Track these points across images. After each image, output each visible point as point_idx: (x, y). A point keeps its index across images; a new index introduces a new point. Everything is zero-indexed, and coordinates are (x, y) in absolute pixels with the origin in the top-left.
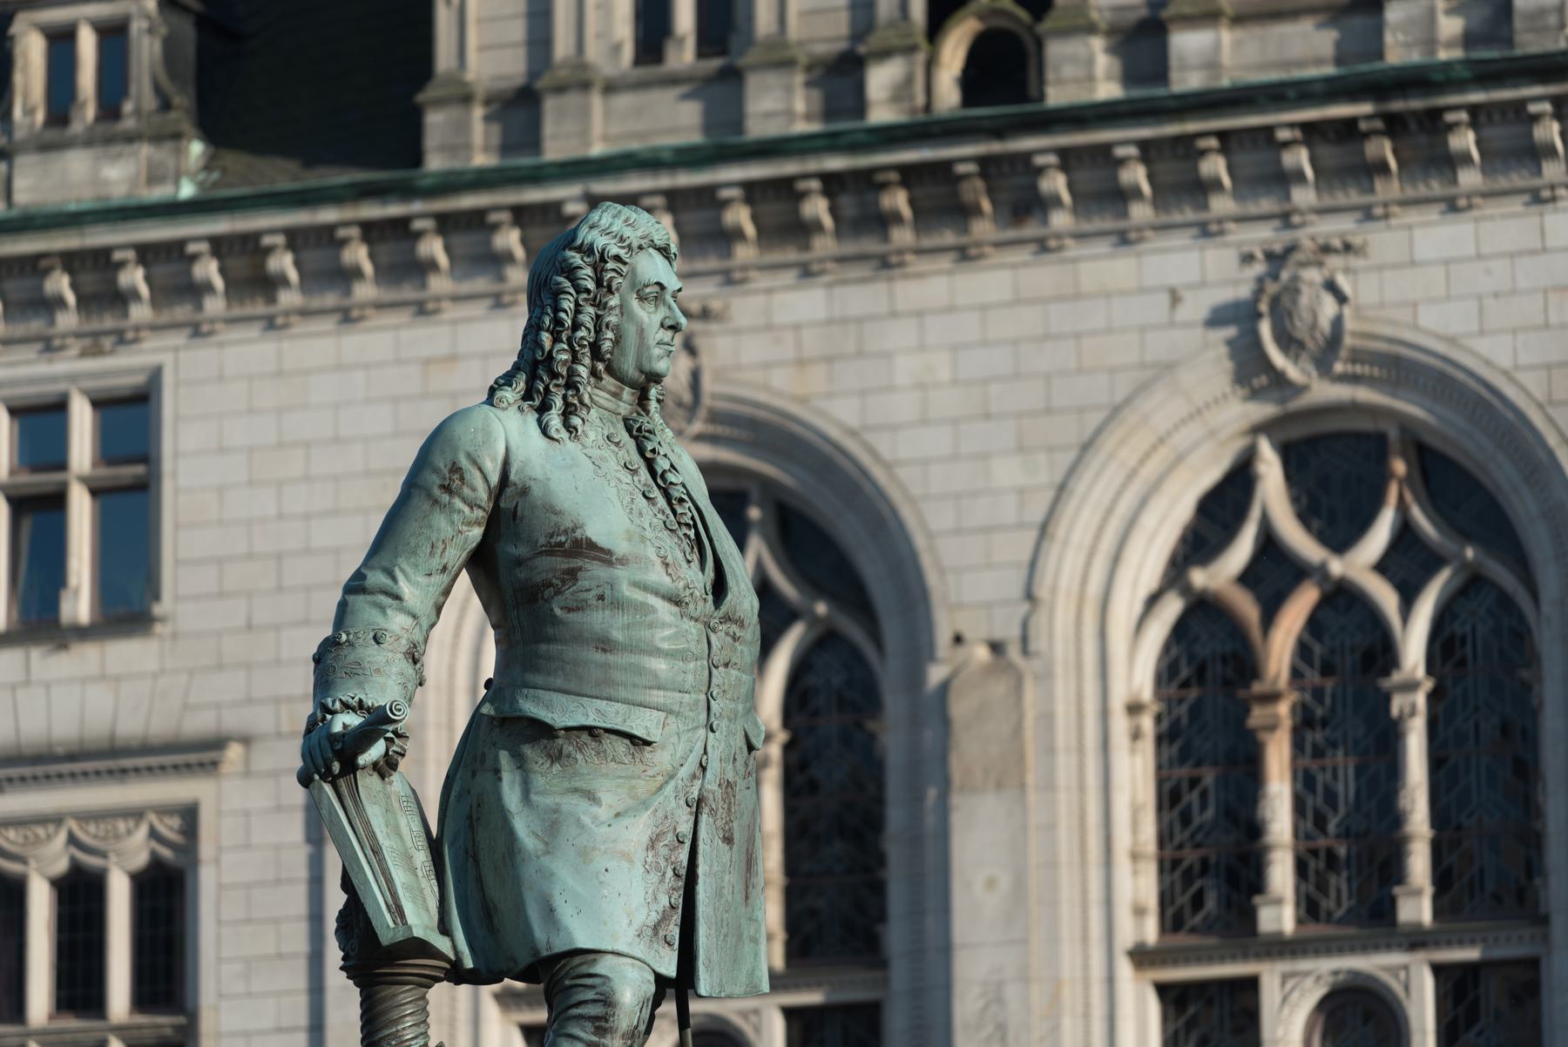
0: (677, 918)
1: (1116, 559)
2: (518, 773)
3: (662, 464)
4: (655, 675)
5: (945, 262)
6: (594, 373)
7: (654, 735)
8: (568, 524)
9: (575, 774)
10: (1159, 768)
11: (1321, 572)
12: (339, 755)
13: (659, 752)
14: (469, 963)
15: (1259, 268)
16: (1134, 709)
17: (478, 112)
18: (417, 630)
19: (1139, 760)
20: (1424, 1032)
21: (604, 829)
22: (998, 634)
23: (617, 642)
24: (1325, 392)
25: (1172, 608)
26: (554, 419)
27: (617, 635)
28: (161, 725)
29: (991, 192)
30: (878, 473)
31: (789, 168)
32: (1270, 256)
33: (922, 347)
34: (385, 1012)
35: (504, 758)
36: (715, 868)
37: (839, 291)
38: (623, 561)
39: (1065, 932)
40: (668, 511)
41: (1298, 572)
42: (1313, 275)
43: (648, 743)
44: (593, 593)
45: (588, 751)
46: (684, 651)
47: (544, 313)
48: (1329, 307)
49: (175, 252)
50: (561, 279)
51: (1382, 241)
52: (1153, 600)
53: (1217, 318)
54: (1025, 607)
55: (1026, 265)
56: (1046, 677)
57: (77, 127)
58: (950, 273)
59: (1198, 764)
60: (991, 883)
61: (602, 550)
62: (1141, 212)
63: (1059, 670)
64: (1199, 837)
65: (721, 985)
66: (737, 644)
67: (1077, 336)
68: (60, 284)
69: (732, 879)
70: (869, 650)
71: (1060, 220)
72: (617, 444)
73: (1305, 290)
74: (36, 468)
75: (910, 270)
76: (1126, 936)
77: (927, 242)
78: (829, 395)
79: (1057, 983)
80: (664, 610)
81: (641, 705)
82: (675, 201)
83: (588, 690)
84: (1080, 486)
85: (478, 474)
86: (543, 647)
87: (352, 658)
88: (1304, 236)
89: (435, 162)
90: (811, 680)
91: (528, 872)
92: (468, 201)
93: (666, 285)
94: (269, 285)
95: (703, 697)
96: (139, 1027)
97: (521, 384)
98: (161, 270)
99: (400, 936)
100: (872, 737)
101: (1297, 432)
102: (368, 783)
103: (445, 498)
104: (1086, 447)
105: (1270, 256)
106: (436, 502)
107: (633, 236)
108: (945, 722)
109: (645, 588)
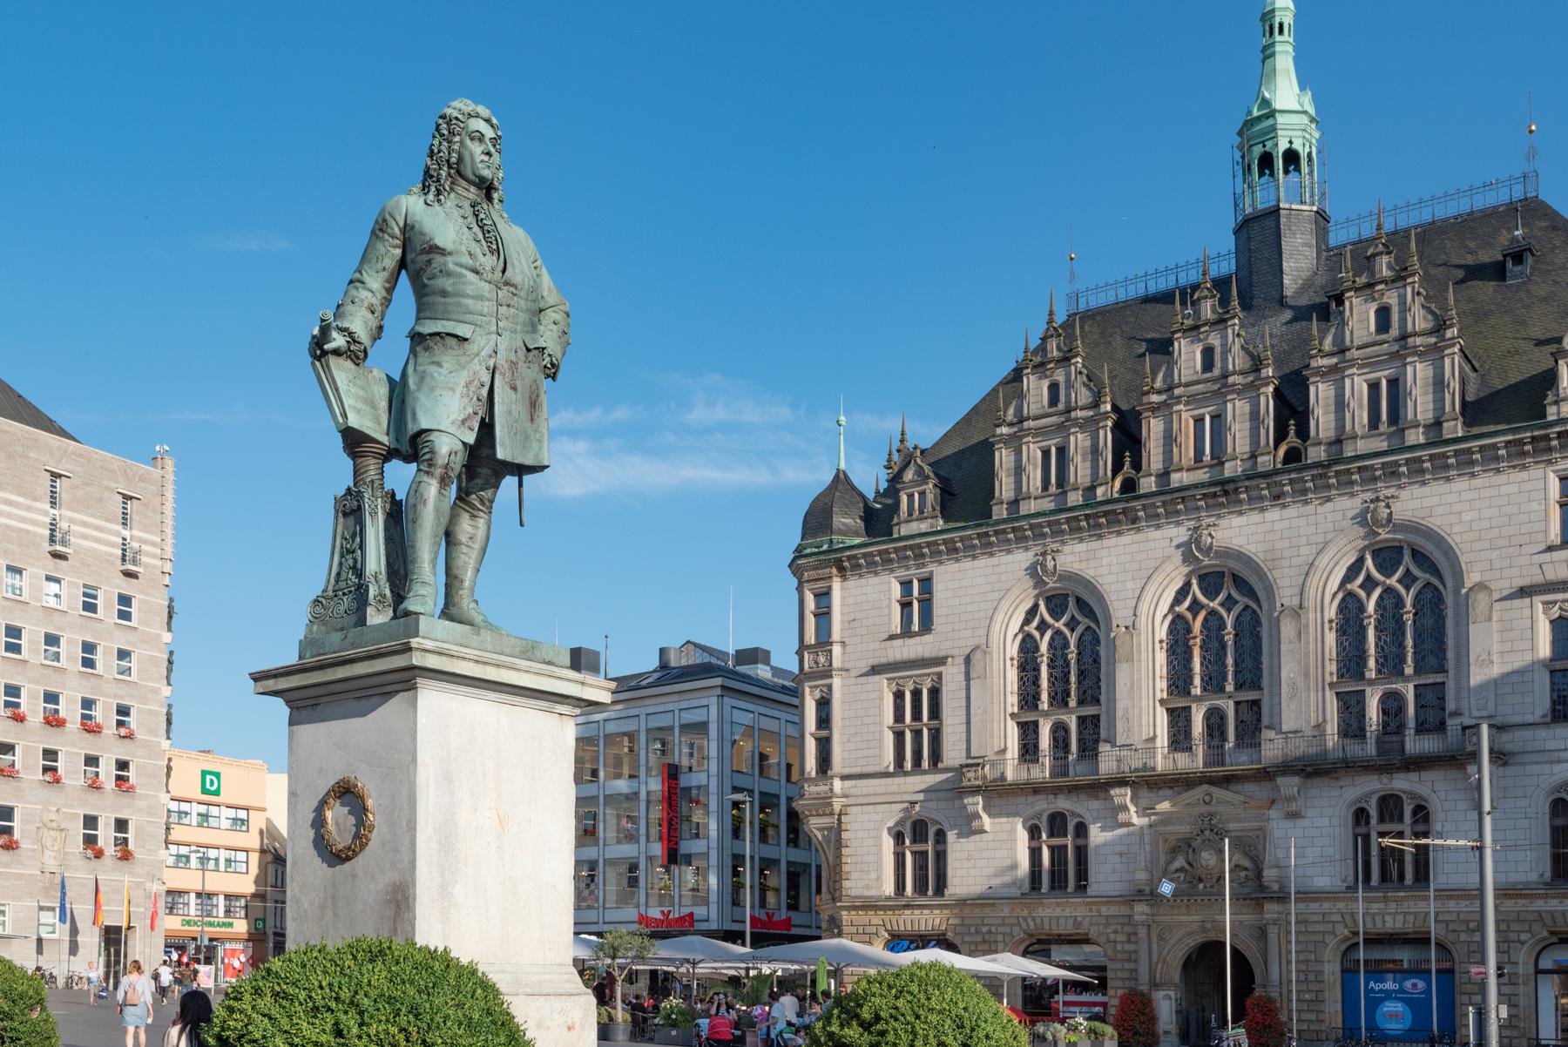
11: (1208, 605)
15: (1190, 533)
17: (1005, 506)
24: (1207, 562)
28: (934, 654)
30: (1099, 587)
41: (1202, 607)
42: (1205, 532)
43: (466, 340)
48: (1209, 540)
51: (1223, 523)
53: (1178, 547)
56: (1139, 635)
57: (914, 516)
60: (1125, 684)
76: (1159, 696)
83: (439, 316)
84: (1147, 588)
86: (425, 299)
88: (1203, 523)
89: (994, 518)
90: (1083, 638)
95: (494, 320)
108: (1115, 646)
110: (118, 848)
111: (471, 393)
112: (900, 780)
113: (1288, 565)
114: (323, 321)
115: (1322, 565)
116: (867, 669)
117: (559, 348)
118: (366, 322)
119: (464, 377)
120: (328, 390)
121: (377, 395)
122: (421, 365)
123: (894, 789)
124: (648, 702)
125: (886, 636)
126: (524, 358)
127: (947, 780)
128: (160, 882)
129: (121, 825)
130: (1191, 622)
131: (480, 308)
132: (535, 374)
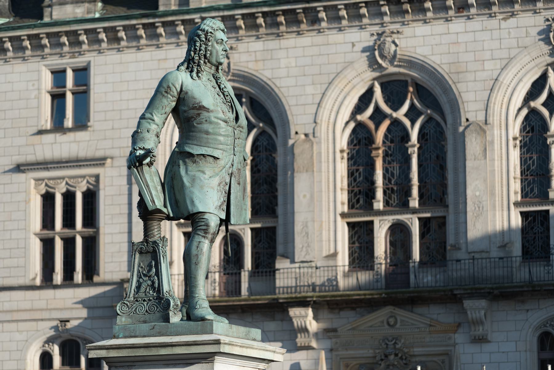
0: (226, 204)
1: (338, 113)
2: (184, 166)
3: (222, 86)
4: (220, 141)
5: (294, 35)
6: (205, 62)
7: (220, 157)
8: (198, 101)
9: (199, 166)
10: (348, 166)
11: (391, 116)
12: (138, 161)
13: (221, 161)
14: (171, 215)
15: (375, 37)
16: (342, 151)
18: (158, 129)
19: (343, 164)
20: (416, 235)
21: (207, 181)
22: (307, 132)
23: (210, 132)
24: (392, 70)
25: (352, 125)
27: (210, 130)
28: (90, 154)
29: (305, 17)
30: (276, 90)
31: (254, 10)
32: (378, 34)
33: (288, 57)
34: (150, 228)
35: (181, 162)
37: (266, 42)
38: (212, 111)
39: (324, 209)
40: (224, 98)
42: (389, 39)
43: (218, 159)
44: (204, 119)
45: (203, 161)
46: (228, 135)
47: (192, 47)
48: (393, 48)
49: (94, 31)
50: (196, 38)
51: (407, 31)
52: (347, 123)
53: (364, 50)
54: (314, 124)
55: (315, 36)
56: (319, 143)
58: (295, 38)
59: (358, 166)
60: (305, 196)
61: (207, 108)
62: (345, 23)
63: (323, 141)
64: (358, 185)
65: (237, 221)
67: (328, 54)
68: (64, 39)
69: (240, 194)
70: (273, 136)
71: (324, 24)
72: (211, 81)
73: (387, 43)
74: (58, 87)
75: (284, 37)
76: (340, 210)
77: (289, 30)
78: (264, 70)
79: (322, 222)
80: (223, 124)
81: (216, 149)
82: (224, 19)
83: (202, 145)
84: (328, 93)
85: (174, 88)
86: (191, 133)
87: (141, 136)
89: (162, 8)
90: (258, 143)
91: (187, 192)
92: (170, 19)
94: (118, 40)
95: (233, 147)
96: (84, 232)
97: (186, 65)
98: (90, 36)
99: (154, 208)
100: (274, 158)
101: (385, 80)
102: (146, 168)
103: (166, 94)
104: (330, 83)
105: (378, 34)
106: (163, 96)
107: (215, 27)
108: (293, 154)
109: (218, 118)
112: (49, 293)
113: (473, 79)
115: (506, 82)
116: (11, 167)
123: (42, 304)
125: (35, 130)
126: (242, 166)
127: (103, 295)
130: (374, 131)
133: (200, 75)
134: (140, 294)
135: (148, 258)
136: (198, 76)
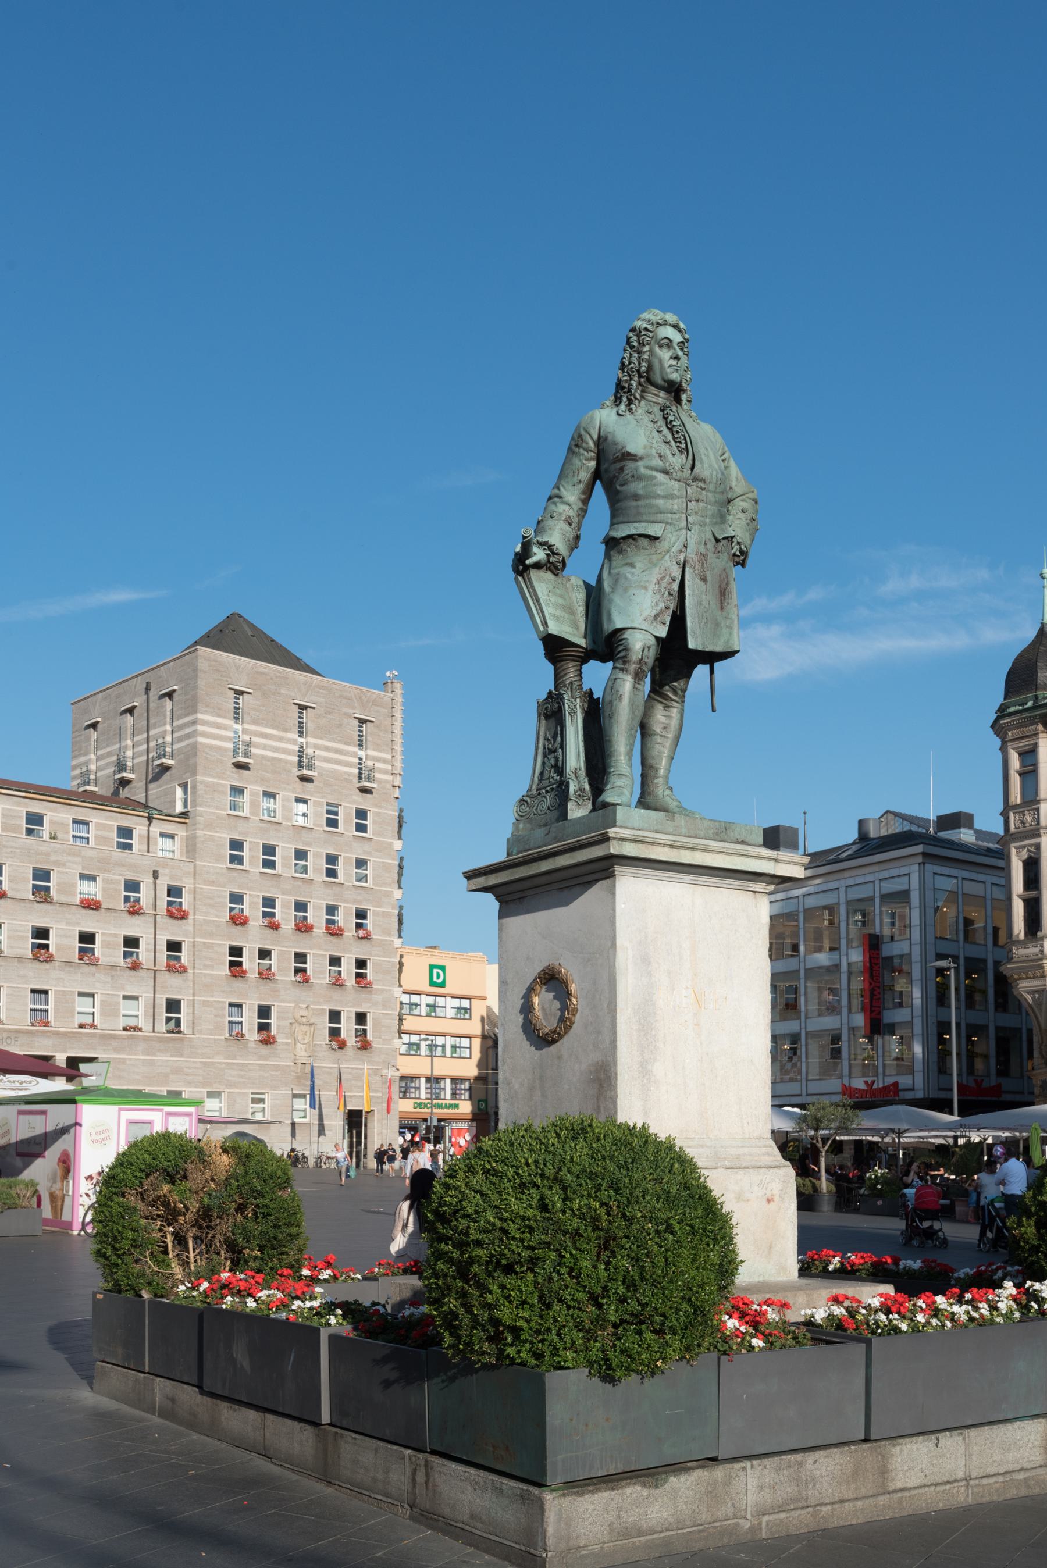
4: (658, 507)
6: (640, 384)
8: (620, 447)
18: (571, 511)
21: (636, 577)
26: (623, 407)
27: (641, 492)
36: (696, 592)
38: (641, 458)
43: (657, 538)
66: (704, 492)
69: (710, 599)
72: (650, 413)
80: (661, 477)
81: (653, 522)
91: (605, 603)
93: (671, 338)
95: (684, 516)
103: (576, 450)
106: (574, 452)
107: (654, 319)
109: (652, 468)
110: (358, 1039)
111: (663, 590)
114: (524, 537)
117: (747, 535)
118: (563, 534)
119: (655, 574)
120: (529, 601)
121: (575, 602)
122: (615, 568)
124: (847, 874)
128: (394, 1069)
129: (361, 1018)
131: (670, 507)
132: (724, 563)
133: (633, 406)
134: (543, 782)
135: (552, 722)
136: (630, 410)
